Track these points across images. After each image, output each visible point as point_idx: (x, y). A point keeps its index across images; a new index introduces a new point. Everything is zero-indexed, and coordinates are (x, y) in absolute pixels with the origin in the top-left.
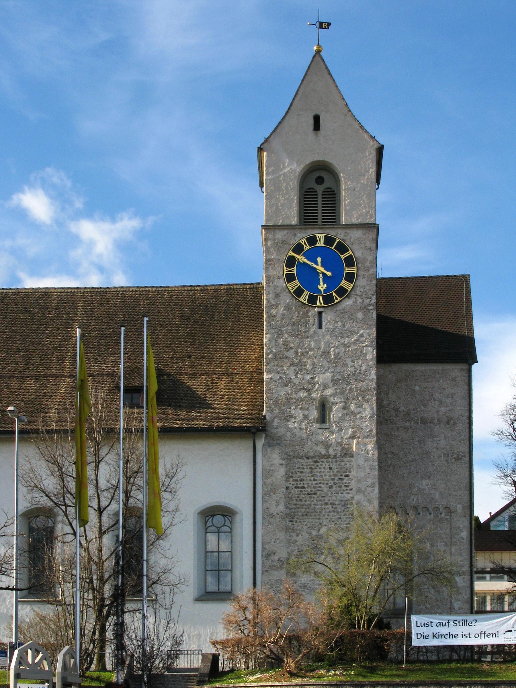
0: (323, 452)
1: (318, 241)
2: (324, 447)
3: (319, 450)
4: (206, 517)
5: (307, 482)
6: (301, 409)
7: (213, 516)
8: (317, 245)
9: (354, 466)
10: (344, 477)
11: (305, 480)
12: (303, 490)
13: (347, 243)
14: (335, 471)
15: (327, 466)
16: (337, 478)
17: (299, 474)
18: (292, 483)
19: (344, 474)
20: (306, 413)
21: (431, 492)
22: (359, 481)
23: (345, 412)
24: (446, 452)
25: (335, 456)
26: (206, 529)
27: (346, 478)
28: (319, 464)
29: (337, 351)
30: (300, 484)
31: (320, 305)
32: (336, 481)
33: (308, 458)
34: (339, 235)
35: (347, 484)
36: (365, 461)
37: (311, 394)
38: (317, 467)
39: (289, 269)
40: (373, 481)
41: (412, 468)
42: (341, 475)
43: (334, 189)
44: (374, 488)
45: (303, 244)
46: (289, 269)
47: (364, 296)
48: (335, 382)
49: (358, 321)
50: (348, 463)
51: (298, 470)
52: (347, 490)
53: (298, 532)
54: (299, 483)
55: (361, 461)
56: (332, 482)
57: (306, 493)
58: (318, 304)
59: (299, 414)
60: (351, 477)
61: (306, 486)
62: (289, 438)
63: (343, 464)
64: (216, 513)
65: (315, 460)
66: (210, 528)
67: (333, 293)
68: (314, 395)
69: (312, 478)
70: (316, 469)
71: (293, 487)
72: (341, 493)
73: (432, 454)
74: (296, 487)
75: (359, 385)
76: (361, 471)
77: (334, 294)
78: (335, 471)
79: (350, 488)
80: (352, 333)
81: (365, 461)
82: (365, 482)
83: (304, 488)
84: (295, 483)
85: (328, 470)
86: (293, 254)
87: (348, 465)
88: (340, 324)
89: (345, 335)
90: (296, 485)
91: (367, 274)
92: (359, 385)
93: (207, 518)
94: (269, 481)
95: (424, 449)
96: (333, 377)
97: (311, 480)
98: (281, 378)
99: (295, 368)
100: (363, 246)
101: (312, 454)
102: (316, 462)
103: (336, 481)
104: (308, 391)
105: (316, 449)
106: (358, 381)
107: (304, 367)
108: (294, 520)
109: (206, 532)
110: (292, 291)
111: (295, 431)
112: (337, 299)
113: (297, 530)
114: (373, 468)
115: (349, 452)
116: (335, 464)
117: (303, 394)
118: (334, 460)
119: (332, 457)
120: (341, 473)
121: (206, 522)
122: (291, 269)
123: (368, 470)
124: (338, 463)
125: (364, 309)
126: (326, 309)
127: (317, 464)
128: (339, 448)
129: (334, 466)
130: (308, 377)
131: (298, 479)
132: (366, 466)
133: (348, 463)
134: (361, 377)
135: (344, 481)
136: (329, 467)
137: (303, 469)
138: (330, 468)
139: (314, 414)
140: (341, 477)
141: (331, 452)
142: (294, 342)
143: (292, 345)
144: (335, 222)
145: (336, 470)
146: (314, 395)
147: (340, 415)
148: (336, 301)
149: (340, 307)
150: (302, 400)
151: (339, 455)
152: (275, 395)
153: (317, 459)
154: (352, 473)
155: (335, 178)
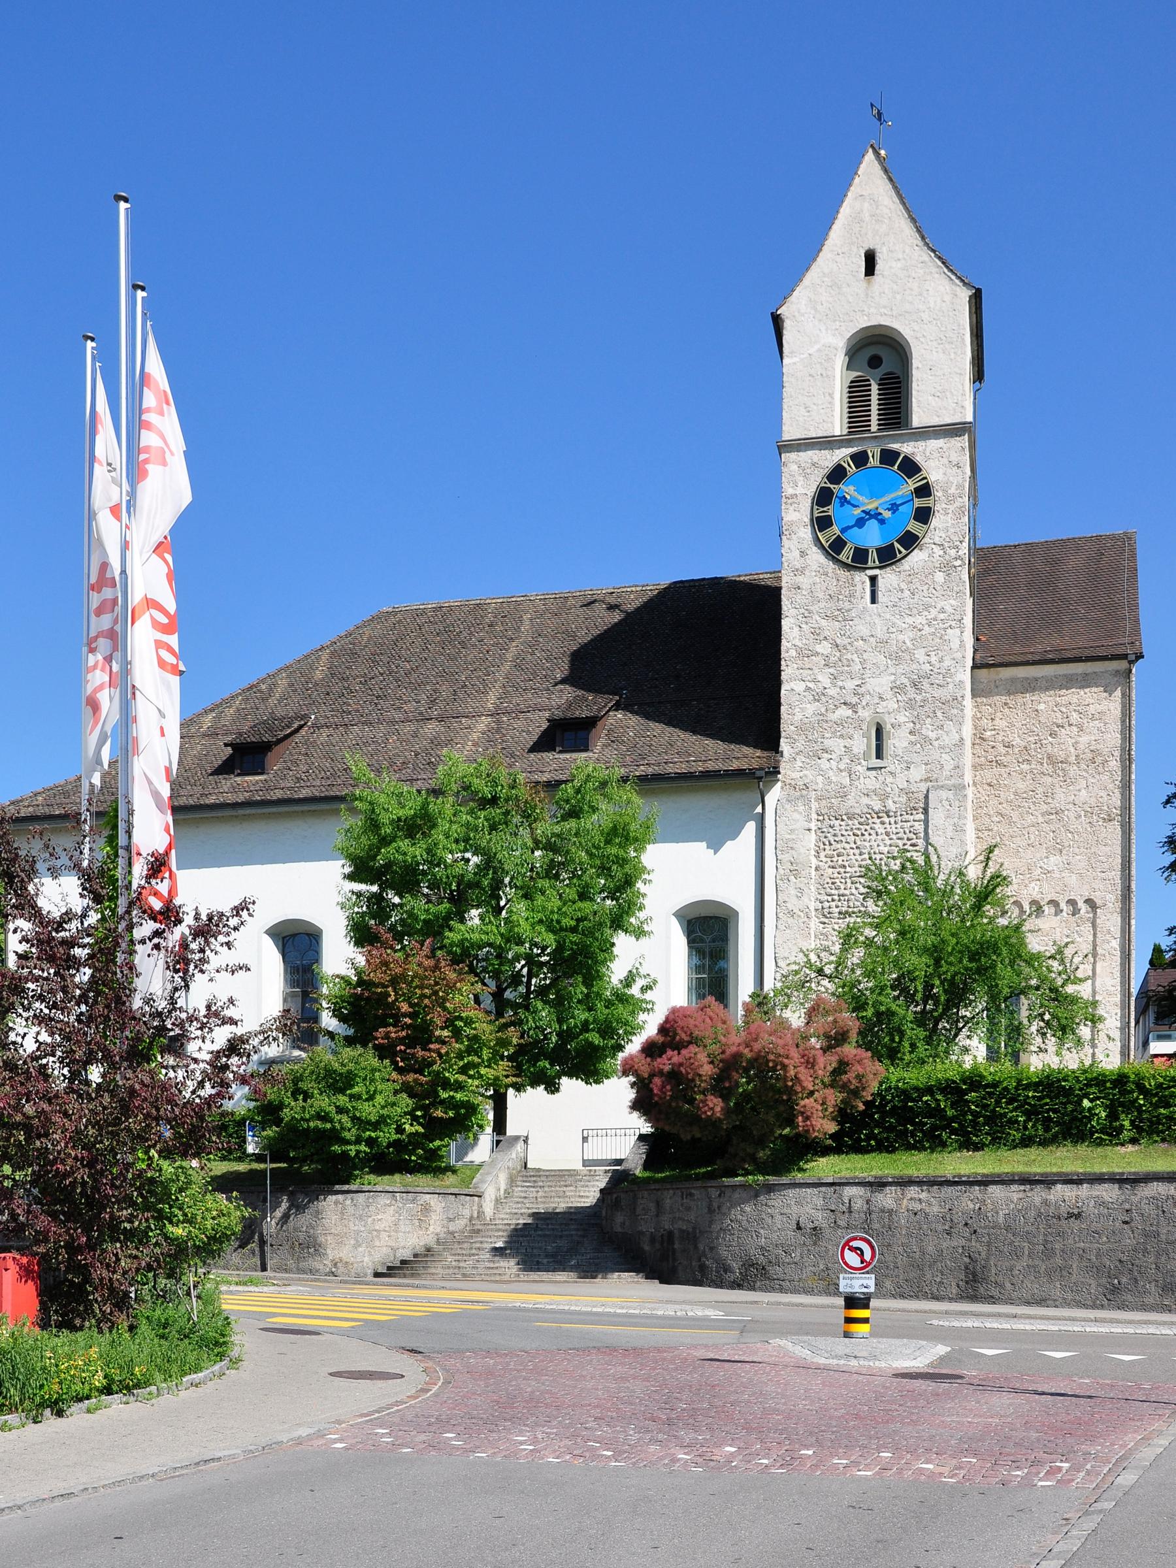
0: (877, 806)
1: (871, 459)
6: (842, 736)
8: (869, 465)
13: (919, 459)
18: (824, 859)
20: (848, 742)
21: (1063, 875)
23: (913, 738)
24: (1089, 809)
29: (901, 637)
31: (873, 565)
34: (906, 448)
37: (856, 712)
39: (822, 509)
41: (1032, 836)
43: (899, 373)
45: (846, 465)
46: (822, 509)
47: (946, 545)
48: (898, 689)
49: (938, 588)
54: (835, 859)
58: (870, 564)
59: (837, 745)
62: (821, 786)
67: (896, 544)
68: (863, 713)
71: (827, 865)
73: (1066, 812)
75: (938, 693)
77: (896, 544)
80: (927, 607)
84: (829, 860)
86: (829, 485)
88: (907, 593)
89: (915, 611)
90: (830, 863)
91: (952, 508)
92: (938, 693)
94: (785, 857)
95: (1052, 806)
96: (894, 681)
98: (808, 689)
99: (832, 670)
100: (945, 461)
104: (853, 707)
106: (935, 686)
107: (846, 668)
110: (826, 545)
111: (831, 773)
112: (900, 552)
116: (894, 826)
117: (845, 712)
122: (825, 509)
125: (947, 567)
126: (882, 572)
128: (904, 799)
130: (850, 684)
134: (939, 680)
139: (861, 743)
141: (891, 806)
142: (830, 628)
143: (827, 633)
144: (899, 423)
146: (863, 713)
147: (906, 744)
148: (899, 556)
149: (906, 564)
150: (839, 723)
152: (798, 717)
155: (896, 350)
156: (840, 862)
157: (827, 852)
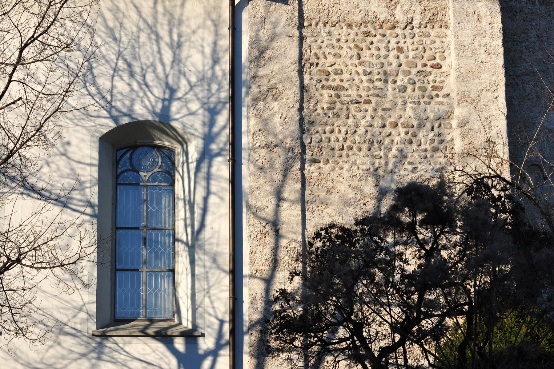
2: (383, 5)
3: (374, 9)
4: (117, 150)
5: (348, 76)
7: (134, 147)
9: (452, 47)
10: (431, 69)
11: (344, 72)
12: (342, 93)
14: (410, 57)
15: (393, 44)
16: (414, 71)
17: (331, 59)
19: (430, 63)
22: (462, 78)
25: (409, 24)
26: (117, 177)
27: (435, 70)
28: (375, 40)
30: (334, 80)
32: (412, 76)
33: (350, 26)
35: (437, 84)
36: (476, 36)
38: (371, 46)
40: (494, 78)
42: (425, 65)
44: (496, 95)
50: (437, 40)
51: (328, 50)
52: (437, 96)
53: (330, 184)
55: (467, 37)
56: (406, 79)
57: (348, 99)
60: (444, 69)
61: (346, 85)
63: (428, 40)
64: (139, 142)
65: (366, 29)
66: (125, 174)
69: (360, 69)
70: (370, 49)
71: (319, 85)
72: (425, 103)
74: (323, 87)
76: (467, 57)
78: (410, 57)
79: (445, 91)
81: (476, 36)
82: (478, 81)
83: (343, 88)
85: (395, 52)
87: (438, 44)
93: (120, 153)
97: (358, 73)
101: (357, 18)
102: (367, 34)
103: (412, 76)
105: (367, 8)
108: (322, 159)
109: (117, 184)
113: (327, 181)
114: (492, 50)
115: (439, 17)
118: (407, 32)
119: (403, 26)
120: (425, 61)
121: (117, 162)
123: (483, 56)
124: (416, 39)
127: (369, 39)
129: (408, 44)
131: (330, 69)
132: (477, 46)
133: (437, 40)
135: (431, 78)
136: (395, 46)
137: (341, 48)
138: (400, 50)
140: (424, 69)
141: (400, 16)
145: (411, 54)
151: (416, 22)
153: (370, 28)
154: (447, 61)
156: (337, 82)
157: (319, 67)
